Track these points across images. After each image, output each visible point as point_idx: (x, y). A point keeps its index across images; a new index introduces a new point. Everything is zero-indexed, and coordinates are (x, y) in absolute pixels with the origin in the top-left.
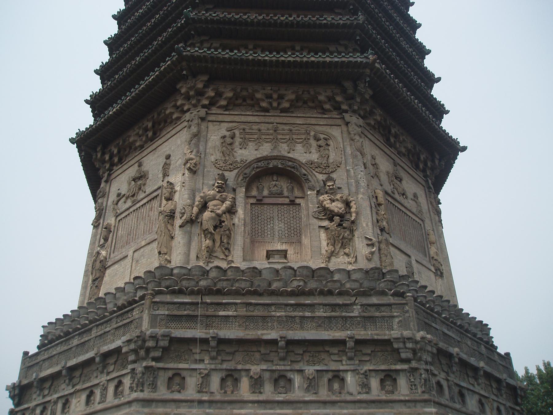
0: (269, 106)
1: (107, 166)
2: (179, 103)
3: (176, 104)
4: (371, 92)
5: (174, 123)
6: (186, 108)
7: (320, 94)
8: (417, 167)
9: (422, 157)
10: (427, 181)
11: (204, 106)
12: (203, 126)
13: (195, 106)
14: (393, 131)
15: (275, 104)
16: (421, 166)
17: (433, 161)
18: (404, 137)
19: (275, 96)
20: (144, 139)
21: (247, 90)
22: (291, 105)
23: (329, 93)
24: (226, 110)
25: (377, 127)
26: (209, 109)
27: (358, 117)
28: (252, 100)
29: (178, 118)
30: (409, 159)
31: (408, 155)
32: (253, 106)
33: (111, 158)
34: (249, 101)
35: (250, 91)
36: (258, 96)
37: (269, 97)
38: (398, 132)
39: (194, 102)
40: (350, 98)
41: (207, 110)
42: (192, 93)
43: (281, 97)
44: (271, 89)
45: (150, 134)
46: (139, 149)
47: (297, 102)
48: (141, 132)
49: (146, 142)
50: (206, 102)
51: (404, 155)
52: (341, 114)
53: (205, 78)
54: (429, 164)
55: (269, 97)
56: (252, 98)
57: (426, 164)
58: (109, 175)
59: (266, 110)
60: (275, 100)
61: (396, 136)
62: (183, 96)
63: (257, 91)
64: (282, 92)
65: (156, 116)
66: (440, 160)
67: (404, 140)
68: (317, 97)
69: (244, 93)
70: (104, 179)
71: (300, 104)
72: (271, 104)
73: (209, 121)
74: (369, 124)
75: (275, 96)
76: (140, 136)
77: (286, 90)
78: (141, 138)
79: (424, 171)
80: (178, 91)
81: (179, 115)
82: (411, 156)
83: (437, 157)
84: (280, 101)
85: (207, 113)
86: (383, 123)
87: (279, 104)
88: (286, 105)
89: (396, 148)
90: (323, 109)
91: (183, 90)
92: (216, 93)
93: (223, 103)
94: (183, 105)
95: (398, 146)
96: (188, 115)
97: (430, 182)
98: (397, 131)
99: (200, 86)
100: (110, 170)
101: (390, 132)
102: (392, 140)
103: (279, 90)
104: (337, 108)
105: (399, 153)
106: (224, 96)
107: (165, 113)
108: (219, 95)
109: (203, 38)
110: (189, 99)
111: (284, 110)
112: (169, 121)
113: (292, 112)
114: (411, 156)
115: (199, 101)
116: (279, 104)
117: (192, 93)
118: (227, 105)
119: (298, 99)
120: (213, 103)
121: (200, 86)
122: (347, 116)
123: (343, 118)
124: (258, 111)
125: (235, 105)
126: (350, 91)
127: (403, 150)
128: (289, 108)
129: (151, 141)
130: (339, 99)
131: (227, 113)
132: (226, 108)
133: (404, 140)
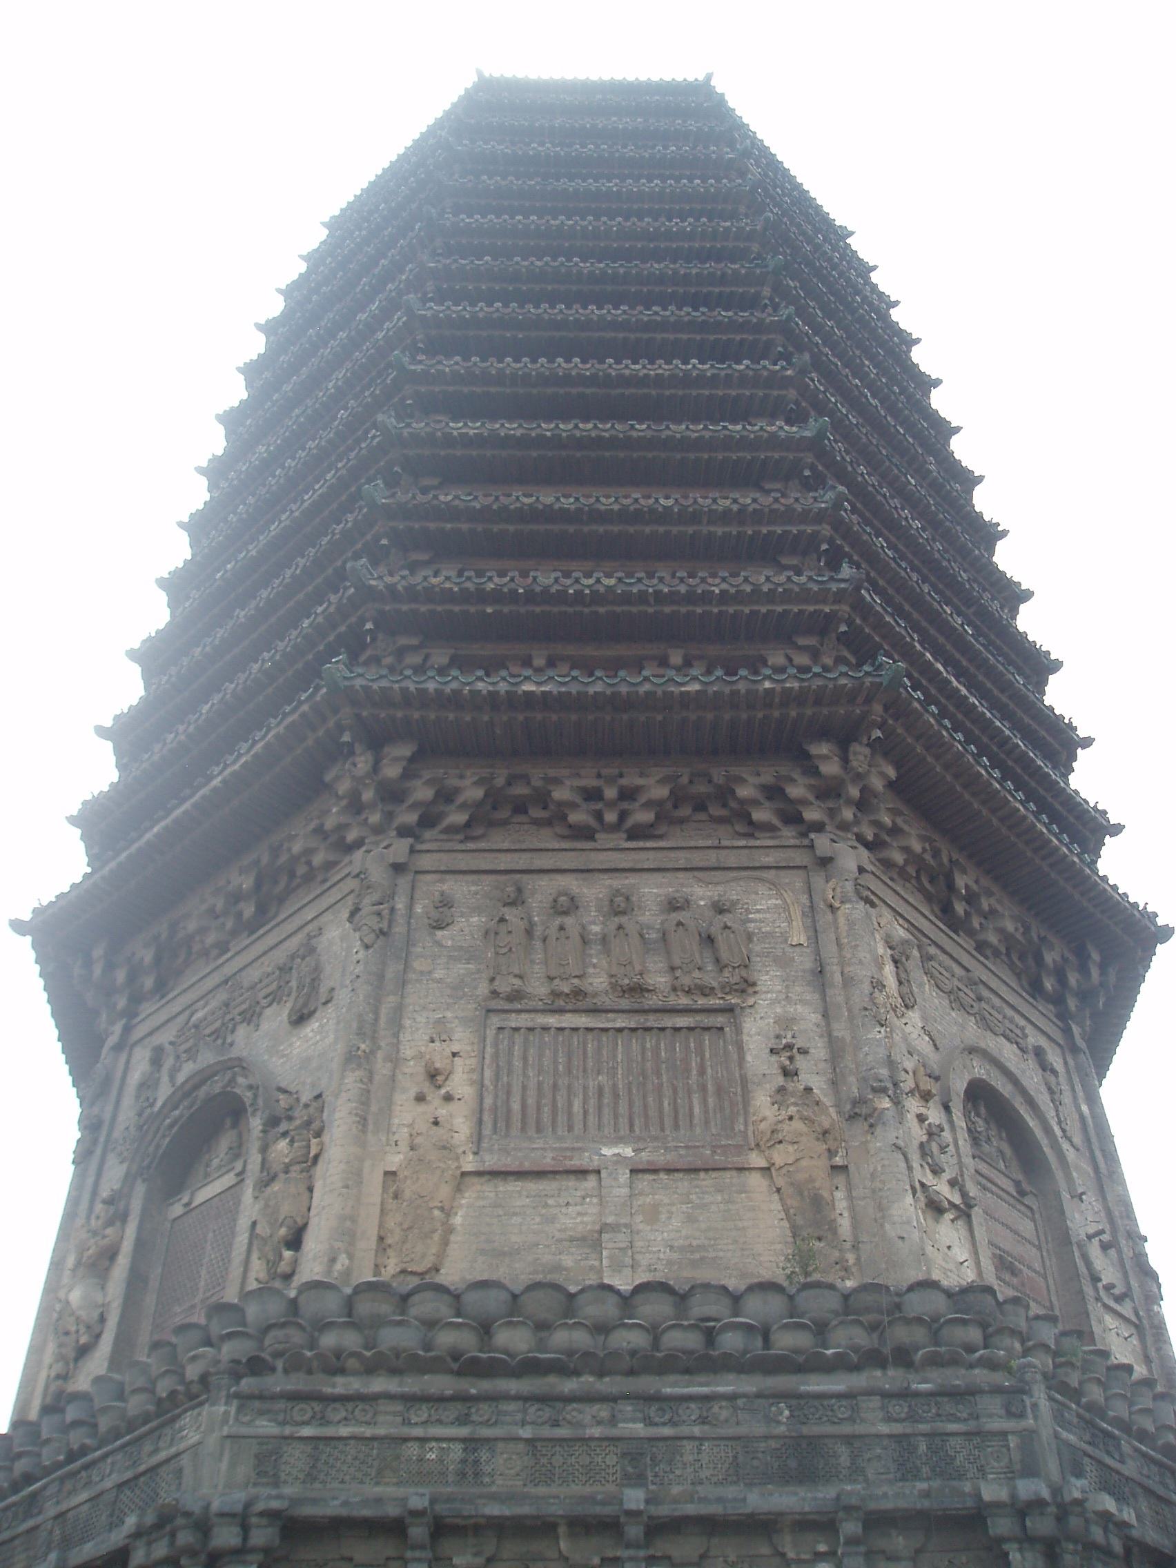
0: (592, 822)
1: (122, 1003)
2: (329, 823)
3: (322, 825)
4: (892, 773)
5: (319, 879)
6: (351, 836)
7: (741, 780)
8: (1035, 988)
9: (1049, 958)
10: (1067, 1031)
11: (403, 832)
12: (404, 882)
13: (378, 830)
14: (961, 881)
15: (611, 817)
16: (1048, 984)
17: (1084, 970)
18: (992, 901)
19: (610, 793)
20: (229, 924)
21: (525, 778)
22: (658, 817)
23: (767, 778)
24: (468, 838)
25: (911, 871)
26: (417, 838)
27: (856, 844)
29: (329, 866)
30: (1012, 966)
31: (1008, 955)
32: (548, 823)
33: (132, 978)
34: (536, 813)
35: (536, 783)
36: (560, 794)
37: (592, 795)
38: (975, 887)
39: (375, 818)
40: (829, 792)
41: (410, 840)
43: (628, 794)
44: (599, 776)
45: (249, 910)
46: (215, 952)
47: (676, 807)
48: (220, 904)
49: (234, 933)
50: (411, 818)
51: (996, 953)
52: (804, 835)
54: (1073, 979)
55: (592, 795)
56: (542, 799)
57: (1062, 980)
58: (127, 1030)
59: (584, 833)
60: (611, 804)
61: (971, 899)
62: (344, 803)
63: (557, 781)
64: (632, 779)
65: (265, 859)
66: (1103, 967)
67: (993, 911)
68: (733, 792)
69: (520, 790)
70: (112, 1040)
71: (685, 811)
72: (599, 816)
73: (417, 872)
75: (610, 793)
76: (217, 917)
77: (642, 775)
78: (221, 920)
79: (1057, 1000)
80: (328, 787)
81: (331, 858)
82: (1015, 958)
83: (1096, 956)
84: (625, 805)
85: (412, 851)
86: (932, 862)
87: (623, 815)
89: (971, 933)
90: (751, 823)
91: (344, 787)
92: (438, 794)
93: (459, 818)
94: (342, 827)
95: (976, 925)
96: (358, 855)
97: (1076, 1029)
98: (971, 883)
99: (392, 771)
100: (130, 1014)
101: (951, 887)
102: (960, 908)
103: (621, 776)
104: (792, 817)
105: (981, 947)
106: (461, 799)
107: (289, 850)
108: (446, 796)
110: (358, 813)
111: (636, 833)
112: (301, 870)
113: (660, 837)
114: (1015, 958)
115: (389, 816)
116: (623, 815)
118: (468, 825)
119: (677, 798)
120: (428, 820)
121: (392, 771)
124: (563, 837)
125: (492, 824)
127: (993, 938)
128: (652, 825)
129: (252, 932)
130: (796, 791)
131: (471, 846)
132: (466, 831)
133: (993, 911)
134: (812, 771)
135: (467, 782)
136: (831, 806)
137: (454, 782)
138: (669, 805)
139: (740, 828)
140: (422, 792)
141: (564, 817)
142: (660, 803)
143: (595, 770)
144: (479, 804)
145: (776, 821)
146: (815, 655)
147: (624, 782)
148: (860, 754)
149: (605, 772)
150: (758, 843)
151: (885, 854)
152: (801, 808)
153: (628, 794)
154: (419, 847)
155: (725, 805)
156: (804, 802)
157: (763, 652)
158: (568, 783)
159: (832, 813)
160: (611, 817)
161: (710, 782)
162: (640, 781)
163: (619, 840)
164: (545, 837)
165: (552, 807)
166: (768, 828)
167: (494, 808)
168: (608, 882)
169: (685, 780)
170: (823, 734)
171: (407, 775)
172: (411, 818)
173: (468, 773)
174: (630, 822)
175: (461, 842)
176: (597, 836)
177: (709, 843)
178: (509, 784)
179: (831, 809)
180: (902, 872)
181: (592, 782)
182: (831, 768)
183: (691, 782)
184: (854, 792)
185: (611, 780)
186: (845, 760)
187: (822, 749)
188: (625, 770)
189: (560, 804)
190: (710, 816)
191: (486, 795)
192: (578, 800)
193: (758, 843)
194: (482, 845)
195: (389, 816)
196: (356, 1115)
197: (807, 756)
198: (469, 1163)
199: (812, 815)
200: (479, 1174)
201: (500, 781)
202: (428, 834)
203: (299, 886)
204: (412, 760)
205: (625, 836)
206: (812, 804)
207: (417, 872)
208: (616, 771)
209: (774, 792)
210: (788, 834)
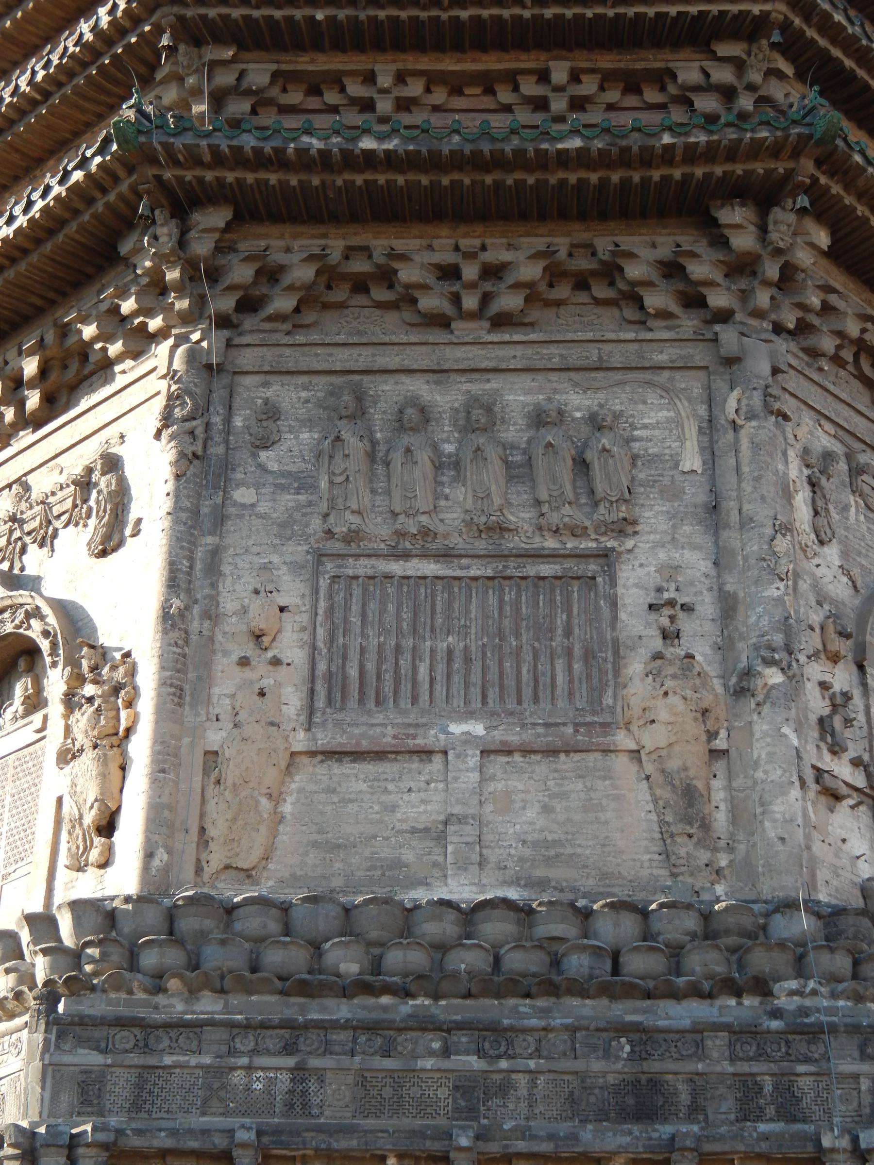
0: (447, 308)
15: (470, 302)
19: (470, 272)
21: (366, 250)
22: (527, 300)
23: (664, 252)
28: (391, 287)
32: (394, 306)
40: (742, 267)
42: (172, 275)
45: (33, 400)
47: (551, 285)
53: (216, 218)
64: (498, 253)
68: (621, 270)
72: (456, 300)
73: (235, 373)
74: (814, 353)
75: (470, 272)
77: (510, 247)
84: (488, 286)
85: (229, 344)
87: (486, 299)
88: (510, 302)
99: (202, 247)
103: (484, 248)
104: (693, 300)
106: (287, 280)
108: (271, 274)
109: (211, 53)
111: (501, 321)
116: (486, 299)
117: (172, 275)
120: (249, 304)
121: (202, 247)
122: (728, 335)
123: (715, 340)
126: (743, 241)
130: (698, 270)
134: (721, 242)
135: (294, 258)
136: (743, 287)
137: (280, 258)
138: (543, 287)
139: (630, 313)
140: (241, 273)
141: (414, 301)
142: (530, 285)
143: (453, 241)
144: (309, 287)
145: (674, 307)
146: (740, 65)
147: (488, 257)
148: (783, 219)
149: (464, 243)
150: (649, 336)
151: (811, 341)
152: (705, 291)
153: (493, 272)
154: (237, 341)
155: (612, 284)
156: (711, 284)
157: (671, 65)
158: (417, 258)
159: (745, 296)
160: (470, 302)
161: (594, 254)
162: (506, 256)
163: (479, 330)
164: (391, 326)
165: (399, 289)
166: (664, 315)
167: (329, 287)
168: (465, 387)
169: (563, 254)
170: (737, 191)
171: (220, 249)
172: (227, 304)
173: (296, 245)
174: (494, 308)
175: (288, 333)
176: (454, 325)
177: (590, 335)
178: (347, 258)
179: (743, 291)
180: (837, 360)
181: (447, 257)
182: (743, 241)
183: (570, 255)
184: (772, 271)
185: (470, 256)
186: (763, 229)
187: (733, 214)
188: (488, 241)
189: (408, 286)
190: (595, 298)
191: (318, 273)
192: (431, 280)
193: (649, 336)
194: (315, 337)
195: (200, 302)
196: (171, 685)
197: (714, 222)
198: (300, 741)
199: (718, 300)
200: (312, 754)
201: (335, 256)
202: (249, 322)
203: (92, 373)
204: (228, 227)
205: (487, 325)
206: (719, 285)
207: (235, 373)
208: (477, 242)
209: (672, 269)
210: (689, 323)
